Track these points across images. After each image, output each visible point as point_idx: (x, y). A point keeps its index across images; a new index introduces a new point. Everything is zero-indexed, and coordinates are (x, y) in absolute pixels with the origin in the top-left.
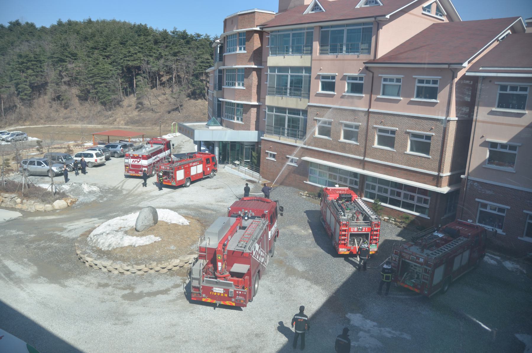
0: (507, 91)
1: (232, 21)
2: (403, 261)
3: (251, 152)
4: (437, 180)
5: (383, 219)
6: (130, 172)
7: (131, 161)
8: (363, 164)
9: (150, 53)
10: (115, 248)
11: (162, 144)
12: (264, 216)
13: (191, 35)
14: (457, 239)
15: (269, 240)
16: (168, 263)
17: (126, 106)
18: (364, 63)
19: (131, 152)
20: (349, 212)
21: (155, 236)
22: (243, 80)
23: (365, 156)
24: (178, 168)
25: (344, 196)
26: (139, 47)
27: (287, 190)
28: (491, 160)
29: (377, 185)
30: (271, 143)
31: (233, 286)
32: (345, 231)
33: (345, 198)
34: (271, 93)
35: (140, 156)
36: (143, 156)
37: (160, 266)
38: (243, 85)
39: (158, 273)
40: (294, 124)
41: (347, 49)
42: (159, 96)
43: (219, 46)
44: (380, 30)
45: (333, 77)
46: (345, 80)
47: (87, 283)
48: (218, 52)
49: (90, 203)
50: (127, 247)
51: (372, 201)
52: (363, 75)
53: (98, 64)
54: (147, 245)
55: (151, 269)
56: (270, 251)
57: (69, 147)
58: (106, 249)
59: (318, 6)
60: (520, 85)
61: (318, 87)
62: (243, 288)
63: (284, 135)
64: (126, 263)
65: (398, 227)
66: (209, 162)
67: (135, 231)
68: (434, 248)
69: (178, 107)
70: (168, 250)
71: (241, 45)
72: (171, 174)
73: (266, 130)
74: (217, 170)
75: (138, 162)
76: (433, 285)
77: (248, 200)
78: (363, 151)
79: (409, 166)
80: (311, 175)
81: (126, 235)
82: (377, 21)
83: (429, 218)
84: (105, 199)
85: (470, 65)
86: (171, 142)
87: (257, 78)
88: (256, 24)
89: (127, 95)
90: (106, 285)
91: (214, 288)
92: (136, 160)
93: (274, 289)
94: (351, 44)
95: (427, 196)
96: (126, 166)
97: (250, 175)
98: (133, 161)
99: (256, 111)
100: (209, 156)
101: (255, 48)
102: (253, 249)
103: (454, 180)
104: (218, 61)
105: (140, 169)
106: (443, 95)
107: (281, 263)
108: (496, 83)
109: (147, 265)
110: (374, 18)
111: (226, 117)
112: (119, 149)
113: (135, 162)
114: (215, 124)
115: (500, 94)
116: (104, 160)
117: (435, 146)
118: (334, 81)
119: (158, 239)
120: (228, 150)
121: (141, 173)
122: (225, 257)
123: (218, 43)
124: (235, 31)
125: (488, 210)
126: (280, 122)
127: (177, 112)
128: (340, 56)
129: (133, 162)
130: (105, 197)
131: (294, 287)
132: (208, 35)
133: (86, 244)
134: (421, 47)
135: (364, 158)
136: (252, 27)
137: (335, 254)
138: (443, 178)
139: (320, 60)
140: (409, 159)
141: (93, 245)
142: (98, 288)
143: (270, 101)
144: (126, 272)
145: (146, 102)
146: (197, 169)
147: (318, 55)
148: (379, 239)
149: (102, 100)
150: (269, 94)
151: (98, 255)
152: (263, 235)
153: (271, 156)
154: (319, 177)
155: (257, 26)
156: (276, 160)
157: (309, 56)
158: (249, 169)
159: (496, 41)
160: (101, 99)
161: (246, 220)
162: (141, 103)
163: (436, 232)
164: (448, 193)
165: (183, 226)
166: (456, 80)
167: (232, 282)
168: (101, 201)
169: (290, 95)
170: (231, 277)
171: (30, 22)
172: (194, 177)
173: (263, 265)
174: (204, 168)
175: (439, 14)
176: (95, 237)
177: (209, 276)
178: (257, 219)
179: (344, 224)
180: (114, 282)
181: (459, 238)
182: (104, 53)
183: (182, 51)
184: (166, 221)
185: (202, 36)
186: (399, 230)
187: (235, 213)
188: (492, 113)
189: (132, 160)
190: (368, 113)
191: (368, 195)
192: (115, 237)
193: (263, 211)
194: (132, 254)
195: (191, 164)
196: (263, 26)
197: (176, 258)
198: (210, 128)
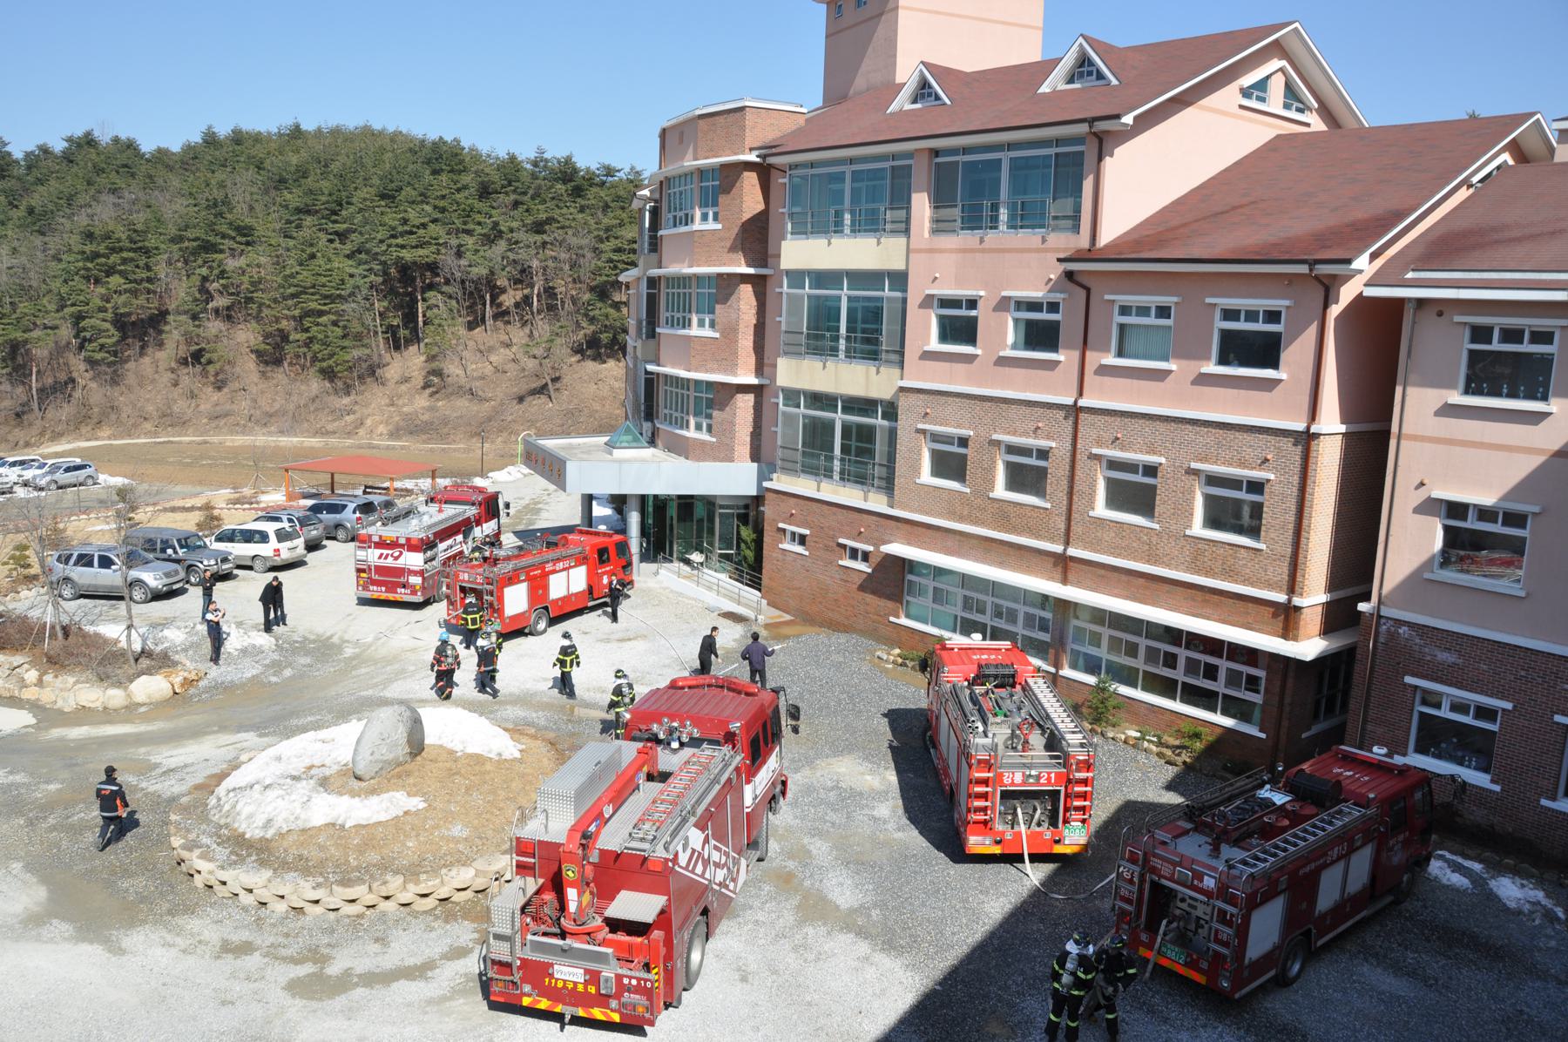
0: (1490, 342)
1: (682, 134)
2: (1153, 883)
3: (738, 526)
4: (1286, 618)
5: (1123, 737)
6: (371, 588)
7: (373, 556)
8: (1063, 566)
9: (465, 223)
10: (284, 831)
11: (473, 504)
12: (730, 738)
13: (588, 169)
14: (1331, 811)
15: (747, 810)
16: (438, 881)
17: (393, 381)
18: (1059, 260)
19: (377, 530)
20: (1002, 722)
21: (409, 795)
22: (711, 311)
23: (1067, 543)
24: (510, 579)
25: (992, 671)
26: (435, 207)
27: (840, 644)
28: (1446, 558)
29: (1106, 632)
30: (793, 501)
31: (614, 962)
32: (985, 782)
33: (996, 677)
34: (793, 351)
35: (402, 541)
36: (408, 540)
37: (413, 889)
38: (712, 325)
39: (407, 909)
40: (860, 443)
41: (1012, 217)
42: (491, 349)
43: (648, 207)
44: (1108, 158)
45: (972, 304)
46: (1007, 310)
47: (188, 942)
48: (647, 225)
49: (243, 685)
50: (319, 829)
51: (1091, 680)
52: (1058, 297)
53: (313, 256)
54: (380, 823)
55: (387, 898)
56: (753, 844)
57: (208, 507)
58: (258, 834)
59: (930, 87)
60: (1530, 326)
61: (925, 331)
62: (647, 967)
63: (831, 477)
64: (311, 879)
65: (1169, 763)
66: (608, 559)
67: (351, 780)
68: (1254, 841)
69: (546, 384)
70: (442, 838)
71: (707, 206)
72: (489, 598)
73: (780, 462)
74: (631, 583)
75: (396, 558)
76: (1247, 961)
77: (690, 687)
78: (1062, 526)
79: (1198, 572)
80: (909, 598)
81: (322, 789)
82: (1095, 134)
83: (1263, 736)
84: (288, 673)
85: (1379, 262)
86: (500, 496)
87: (755, 304)
88: (749, 142)
89: (397, 348)
90: (245, 949)
91: (556, 967)
92: (390, 552)
93: (753, 967)
94: (1023, 203)
95: (1254, 664)
96: (359, 571)
97: (731, 599)
98: (382, 555)
99: (752, 404)
100: (607, 539)
101: (747, 216)
102: (680, 848)
103: (1338, 616)
104: (646, 251)
105: (402, 580)
106: (1296, 354)
107: (786, 880)
108: (1457, 319)
109: (375, 886)
110: (1087, 124)
111: (665, 420)
112: (349, 516)
113: (386, 558)
114: (635, 443)
115: (1471, 352)
116: (301, 550)
117: (1278, 513)
118: (973, 313)
119: (416, 803)
120: (672, 517)
121: (403, 590)
122: (589, 871)
123: (646, 200)
124: (690, 163)
125: (1445, 713)
126: (818, 435)
127: (543, 398)
128: (991, 236)
129: (380, 557)
130: (290, 665)
131: (818, 959)
132: (638, 169)
133: (204, 818)
134: (1235, 208)
135: (1065, 550)
136: (736, 154)
137: (959, 854)
138: (1304, 611)
139: (931, 251)
140: (1199, 554)
141: (222, 822)
142: (219, 957)
143: (794, 373)
144: (309, 908)
145: (453, 369)
146: (568, 582)
147: (926, 235)
148: (1091, 807)
149: (325, 364)
150: (786, 353)
151: (231, 853)
152: (719, 802)
153: (794, 541)
154: (935, 606)
155: (751, 149)
156: (807, 553)
157: (902, 240)
158: (730, 577)
159: (1465, 187)
160: (319, 361)
161: (675, 750)
162: (438, 373)
163: (1268, 786)
164: (1321, 661)
165: (501, 763)
166: (1335, 310)
167: (609, 950)
168: (274, 679)
169: (846, 357)
170: (611, 932)
171: (123, 136)
172: (560, 603)
173: (723, 890)
174: (592, 577)
175: (1296, 104)
176: (232, 794)
177: (543, 928)
178: (707, 750)
179: (980, 761)
180: (271, 939)
181: (1336, 808)
182: (331, 226)
183: (559, 219)
184: (450, 746)
185: (619, 171)
186: (1170, 772)
187: (643, 727)
188: (1448, 410)
189: (378, 552)
190: (1075, 411)
191: (1081, 662)
192: (287, 797)
193: (728, 722)
194: (333, 849)
195: (549, 567)
196: (768, 150)
197: (463, 865)
198: (617, 453)
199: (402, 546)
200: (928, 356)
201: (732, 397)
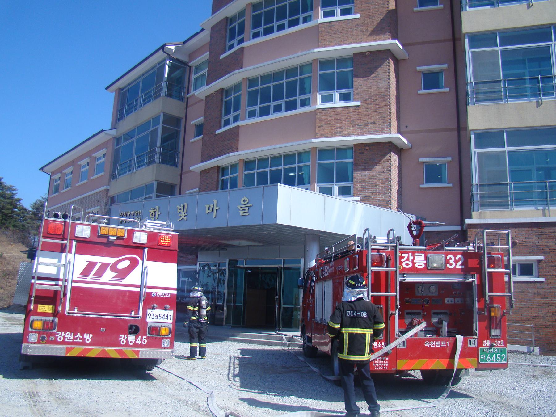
48: (166, 76)
87: (395, 80)
92: (111, 260)
98: (91, 265)
99: (397, 164)
101: (391, 8)
113: (100, 273)
121: (132, 338)
129: (86, 271)
199: (139, 248)
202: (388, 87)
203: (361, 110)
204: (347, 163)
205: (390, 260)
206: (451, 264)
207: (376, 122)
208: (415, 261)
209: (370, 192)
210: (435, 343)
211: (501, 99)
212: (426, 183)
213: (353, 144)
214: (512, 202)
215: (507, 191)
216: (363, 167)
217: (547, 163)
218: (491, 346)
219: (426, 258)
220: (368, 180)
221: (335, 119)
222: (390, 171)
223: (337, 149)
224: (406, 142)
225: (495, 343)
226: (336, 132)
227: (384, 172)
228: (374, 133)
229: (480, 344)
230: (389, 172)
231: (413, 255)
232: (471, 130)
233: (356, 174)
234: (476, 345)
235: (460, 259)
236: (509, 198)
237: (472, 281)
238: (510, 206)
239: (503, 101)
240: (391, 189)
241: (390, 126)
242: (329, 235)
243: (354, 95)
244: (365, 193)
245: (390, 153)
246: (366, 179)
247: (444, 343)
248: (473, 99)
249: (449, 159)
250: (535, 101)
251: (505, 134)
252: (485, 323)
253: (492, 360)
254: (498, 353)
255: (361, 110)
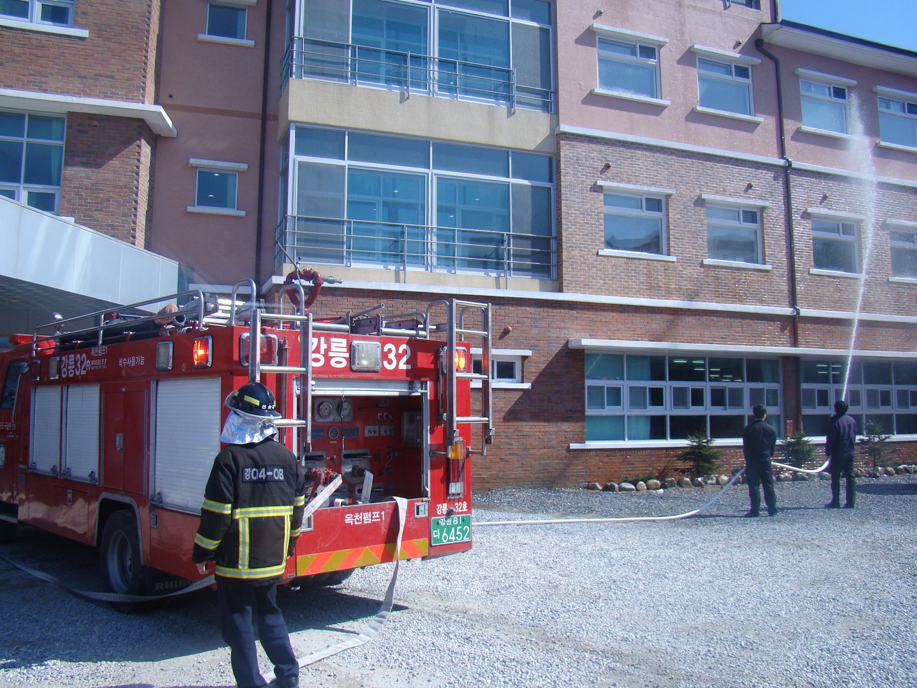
99: (148, 164)
118: (652, 62)
200: (592, 99)
201: (128, 142)
202: (147, 13)
203: (87, 47)
204: (50, 147)
205: (286, 349)
206: (390, 362)
207: (117, 77)
208: (330, 354)
209: (96, 210)
210: (363, 516)
211: (344, 78)
212: (199, 204)
213: (65, 110)
214: (349, 253)
215: (343, 233)
216: (84, 160)
217: (394, 195)
218: (450, 513)
219: (351, 349)
220: (93, 185)
221: (31, 54)
222: (137, 174)
223: (31, 117)
224: (170, 123)
225: (455, 507)
226: (31, 81)
227: (126, 173)
228: (112, 97)
229: (432, 511)
230: (136, 176)
231: (328, 342)
232: (291, 122)
233: (70, 172)
234: (427, 515)
235: (405, 352)
236: (345, 246)
237: (422, 393)
238: (345, 260)
239: (349, 81)
240: (136, 209)
241: (144, 90)
242: (20, 288)
243: (76, 14)
244: (86, 210)
245: (140, 140)
246: (86, 182)
247: (376, 514)
248: (300, 67)
249: (244, 166)
250: (398, 91)
251: (347, 137)
252: (441, 472)
253: (450, 538)
254: (459, 525)
255: (87, 47)
